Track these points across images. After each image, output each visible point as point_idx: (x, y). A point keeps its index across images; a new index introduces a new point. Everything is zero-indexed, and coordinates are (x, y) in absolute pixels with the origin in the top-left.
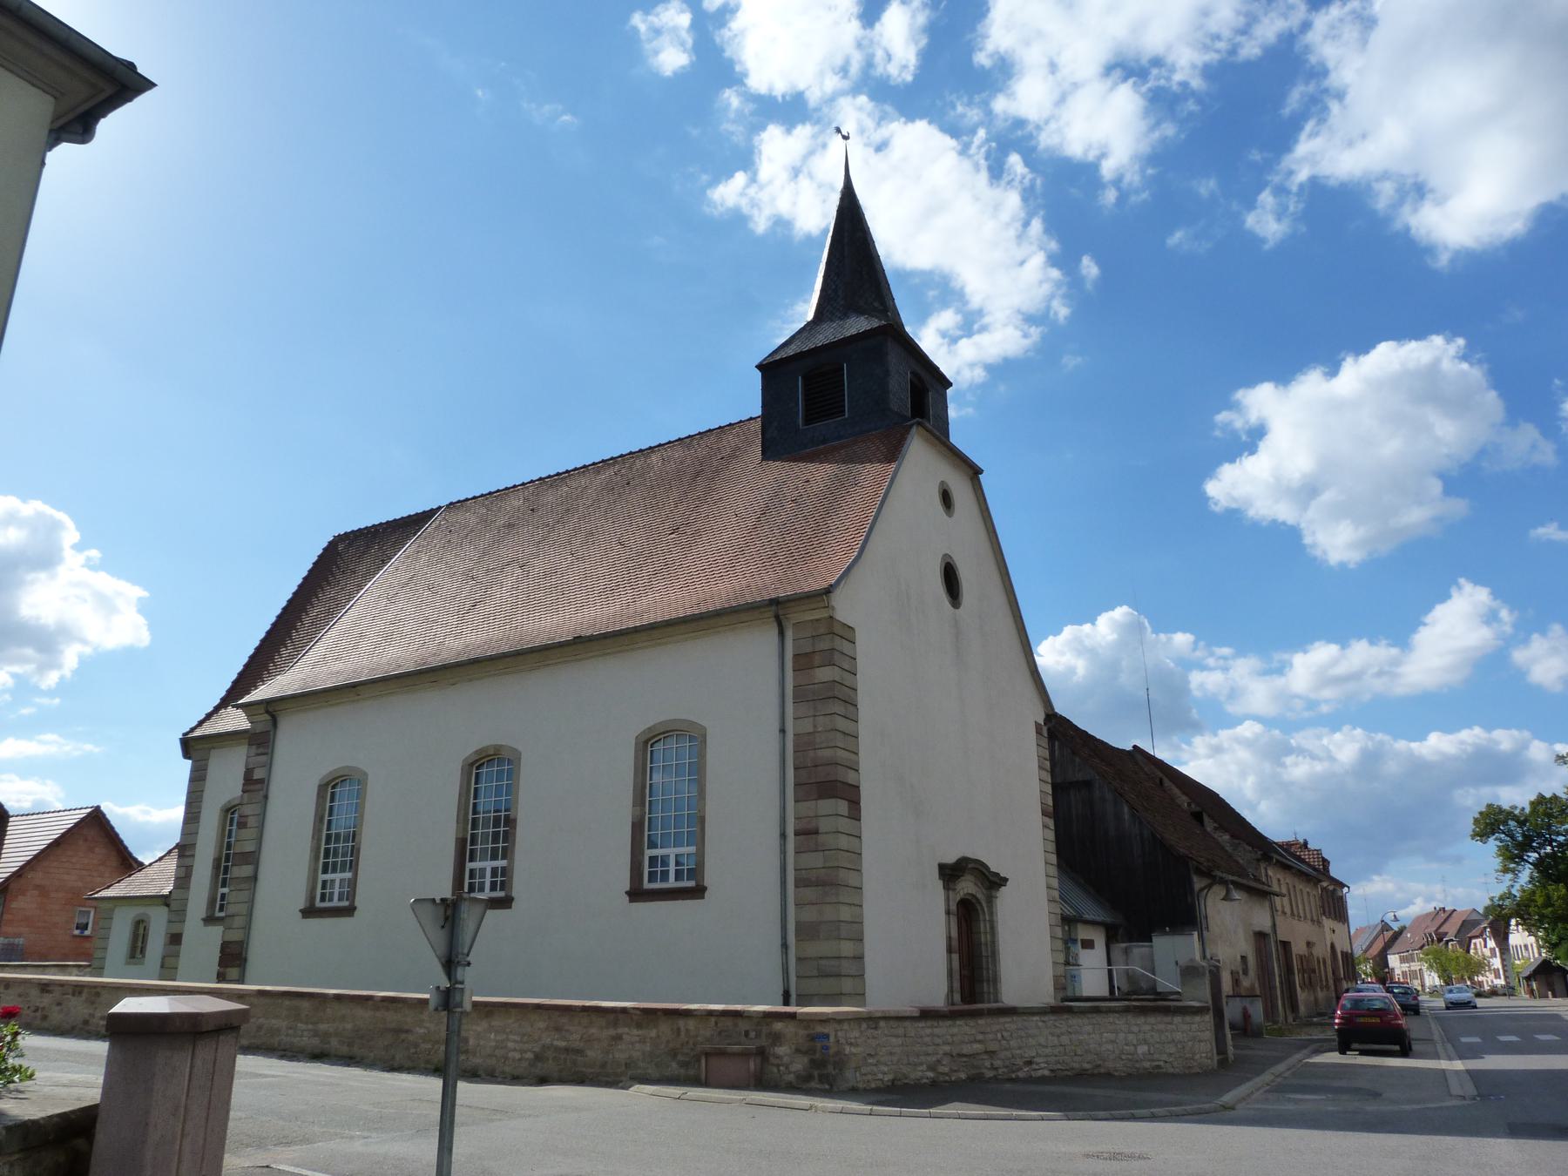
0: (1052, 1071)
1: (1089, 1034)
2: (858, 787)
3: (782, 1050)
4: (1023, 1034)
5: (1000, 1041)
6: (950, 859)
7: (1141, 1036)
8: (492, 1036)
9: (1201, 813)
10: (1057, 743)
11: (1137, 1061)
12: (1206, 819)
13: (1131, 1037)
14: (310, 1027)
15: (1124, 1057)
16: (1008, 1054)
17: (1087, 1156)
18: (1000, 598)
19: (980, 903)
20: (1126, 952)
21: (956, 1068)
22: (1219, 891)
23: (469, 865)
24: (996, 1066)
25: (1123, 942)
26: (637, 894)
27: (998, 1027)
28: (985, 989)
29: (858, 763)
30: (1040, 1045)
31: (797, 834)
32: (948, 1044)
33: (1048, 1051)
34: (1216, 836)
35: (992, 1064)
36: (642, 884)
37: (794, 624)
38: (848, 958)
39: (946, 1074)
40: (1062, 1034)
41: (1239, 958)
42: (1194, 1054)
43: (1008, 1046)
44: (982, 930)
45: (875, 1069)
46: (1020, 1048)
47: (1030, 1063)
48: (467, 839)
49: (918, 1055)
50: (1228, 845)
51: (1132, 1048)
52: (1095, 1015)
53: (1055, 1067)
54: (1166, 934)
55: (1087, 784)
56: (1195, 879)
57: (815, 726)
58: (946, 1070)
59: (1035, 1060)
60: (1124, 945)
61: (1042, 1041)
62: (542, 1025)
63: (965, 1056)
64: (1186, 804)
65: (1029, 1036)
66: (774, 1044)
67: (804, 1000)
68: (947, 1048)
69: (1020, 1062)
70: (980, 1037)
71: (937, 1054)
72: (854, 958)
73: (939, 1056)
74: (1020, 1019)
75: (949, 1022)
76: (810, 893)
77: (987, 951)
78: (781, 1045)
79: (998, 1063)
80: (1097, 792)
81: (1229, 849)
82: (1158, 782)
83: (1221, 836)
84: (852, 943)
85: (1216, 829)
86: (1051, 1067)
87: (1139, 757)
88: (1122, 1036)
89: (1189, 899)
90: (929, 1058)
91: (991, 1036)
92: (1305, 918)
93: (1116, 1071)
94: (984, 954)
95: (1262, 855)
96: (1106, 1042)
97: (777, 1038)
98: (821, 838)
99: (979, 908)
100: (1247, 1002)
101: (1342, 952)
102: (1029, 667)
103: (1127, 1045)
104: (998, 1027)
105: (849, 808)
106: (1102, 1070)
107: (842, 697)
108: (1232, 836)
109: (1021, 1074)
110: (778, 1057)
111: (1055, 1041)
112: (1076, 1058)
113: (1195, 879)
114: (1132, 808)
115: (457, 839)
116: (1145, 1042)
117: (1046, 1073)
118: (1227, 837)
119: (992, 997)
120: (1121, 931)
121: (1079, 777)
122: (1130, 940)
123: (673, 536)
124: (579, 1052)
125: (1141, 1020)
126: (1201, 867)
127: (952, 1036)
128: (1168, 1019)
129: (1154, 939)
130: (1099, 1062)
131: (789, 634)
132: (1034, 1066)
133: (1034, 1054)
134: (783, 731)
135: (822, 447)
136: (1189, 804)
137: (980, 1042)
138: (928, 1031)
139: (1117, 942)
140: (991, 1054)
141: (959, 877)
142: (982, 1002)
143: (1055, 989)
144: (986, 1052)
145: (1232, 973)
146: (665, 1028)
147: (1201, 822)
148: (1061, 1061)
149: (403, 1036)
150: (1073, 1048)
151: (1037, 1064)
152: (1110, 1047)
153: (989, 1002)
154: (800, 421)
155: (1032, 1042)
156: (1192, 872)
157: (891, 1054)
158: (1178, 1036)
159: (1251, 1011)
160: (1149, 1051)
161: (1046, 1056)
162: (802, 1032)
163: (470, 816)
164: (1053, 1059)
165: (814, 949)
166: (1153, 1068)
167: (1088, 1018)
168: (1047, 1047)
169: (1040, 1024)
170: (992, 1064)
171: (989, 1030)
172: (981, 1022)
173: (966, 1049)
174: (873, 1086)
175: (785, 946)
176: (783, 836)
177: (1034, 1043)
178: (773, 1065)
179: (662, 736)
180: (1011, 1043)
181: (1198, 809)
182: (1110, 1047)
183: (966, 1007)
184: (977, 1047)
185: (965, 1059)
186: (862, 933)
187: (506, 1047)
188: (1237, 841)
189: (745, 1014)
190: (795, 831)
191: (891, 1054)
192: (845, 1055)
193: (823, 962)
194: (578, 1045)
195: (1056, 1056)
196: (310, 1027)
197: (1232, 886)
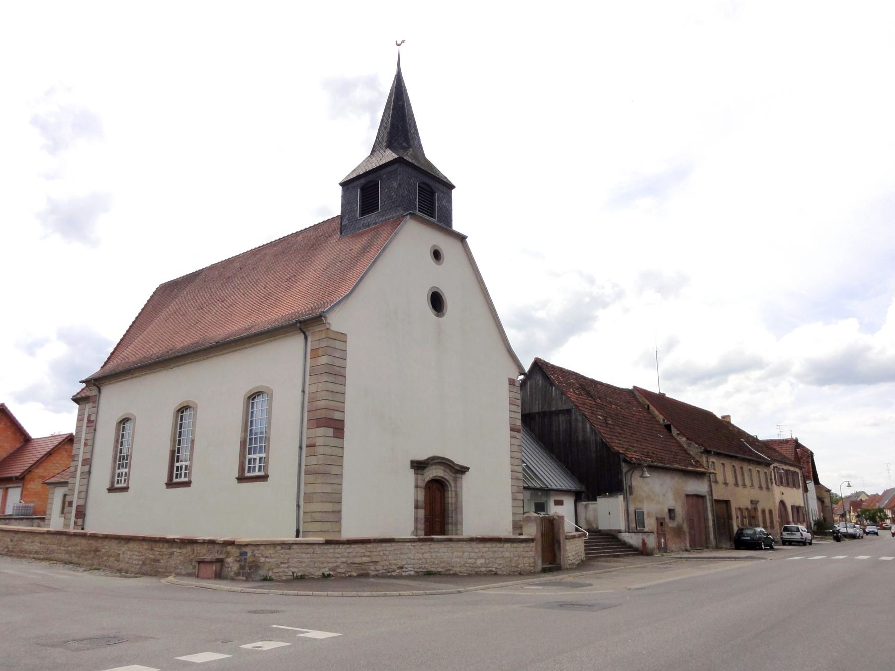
0: (415, 572)
1: (445, 553)
2: (343, 421)
3: (230, 560)
4: (398, 552)
5: (382, 556)
6: (422, 456)
7: (480, 554)
8: (129, 553)
9: (670, 425)
10: (554, 388)
11: (476, 568)
12: (673, 428)
13: (472, 555)
14: (66, 549)
15: (467, 565)
16: (387, 563)
17: (250, 612)
18: (485, 309)
19: (448, 481)
20: (586, 507)
21: (350, 570)
22: (637, 474)
23: (177, 464)
24: (378, 569)
25: (585, 501)
26: (241, 479)
27: (381, 549)
28: (450, 528)
29: (344, 408)
30: (410, 558)
31: (307, 447)
32: (346, 557)
33: (414, 561)
34: (678, 439)
35: (375, 568)
36: (244, 474)
37: (312, 333)
38: (329, 512)
39: (343, 573)
40: (425, 553)
41: (666, 510)
42: (518, 564)
43: (387, 559)
44: (450, 496)
45: (287, 570)
46: (396, 560)
47: (401, 568)
48: (175, 451)
49: (322, 563)
50: (685, 444)
51: (474, 560)
52: (449, 543)
53: (419, 570)
54: (605, 496)
55: (569, 411)
56: (623, 465)
57: (317, 389)
58: (343, 571)
59: (405, 566)
60: (584, 503)
61: (411, 556)
62: (146, 547)
63: (357, 564)
64: (662, 420)
65: (402, 553)
66: (227, 557)
67: (306, 534)
68: (344, 560)
69: (394, 567)
70: (368, 554)
71: (336, 562)
72: (333, 512)
73: (338, 564)
74: (397, 544)
75: (348, 546)
76: (311, 478)
77: (452, 508)
78: (229, 558)
79: (379, 567)
80: (574, 416)
81: (685, 446)
82: (646, 407)
83: (681, 439)
84: (331, 504)
85: (678, 434)
86: (416, 570)
87: (637, 393)
88: (466, 554)
89: (620, 477)
90: (331, 565)
91: (375, 553)
92: (752, 486)
93: (461, 573)
94: (450, 509)
95: (704, 449)
96: (456, 557)
97: (228, 554)
98: (317, 449)
99: (447, 484)
100: (645, 536)
101: (793, 507)
102: (506, 347)
103: (469, 558)
104: (381, 549)
105: (334, 433)
106: (451, 572)
107: (337, 374)
108: (688, 439)
109: (394, 574)
110: (228, 564)
111: (420, 556)
112: (434, 566)
113: (623, 465)
114: (591, 424)
115: (170, 450)
116: (482, 557)
117: (412, 573)
118: (684, 439)
119: (454, 532)
120: (583, 495)
121: (565, 407)
122: (589, 500)
123: (286, 283)
124: (158, 561)
125: (482, 545)
126: (626, 458)
127: (349, 553)
128: (501, 545)
129: (598, 499)
130: (450, 568)
131: (309, 339)
132: (404, 569)
133: (404, 563)
134: (303, 391)
135: (367, 229)
136: (664, 420)
137: (368, 556)
138: (331, 551)
139: (581, 501)
140: (376, 563)
141: (425, 467)
142: (448, 535)
143: (513, 528)
144: (372, 562)
145: (657, 519)
146: (188, 549)
147: (670, 431)
148: (423, 567)
149: (97, 553)
150: (432, 560)
151: (406, 568)
152: (458, 560)
153: (452, 535)
154: (358, 215)
155: (403, 556)
156: (621, 461)
157: (301, 562)
158: (507, 554)
159: (647, 540)
160: (485, 562)
161: (414, 564)
162: (238, 551)
163: (178, 438)
164: (418, 566)
165: (336, 508)
166: (487, 572)
167: (445, 544)
168: (414, 559)
169: (411, 547)
170: (375, 568)
171: (375, 550)
172: (369, 546)
173: (357, 560)
174: (284, 578)
175: (298, 506)
176: (301, 448)
177: (405, 557)
178: (226, 567)
179: (256, 395)
180: (389, 557)
181: (669, 423)
182: (458, 560)
183: (426, 537)
184: (365, 559)
185: (356, 565)
186: (341, 498)
187: (133, 558)
188: (690, 442)
189: (217, 542)
190: (306, 445)
191: (301, 562)
192: (261, 563)
193: (313, 514)
194: (158, 557)
195: (420, 564)
196: (66, 549)
197: (645, 469)
